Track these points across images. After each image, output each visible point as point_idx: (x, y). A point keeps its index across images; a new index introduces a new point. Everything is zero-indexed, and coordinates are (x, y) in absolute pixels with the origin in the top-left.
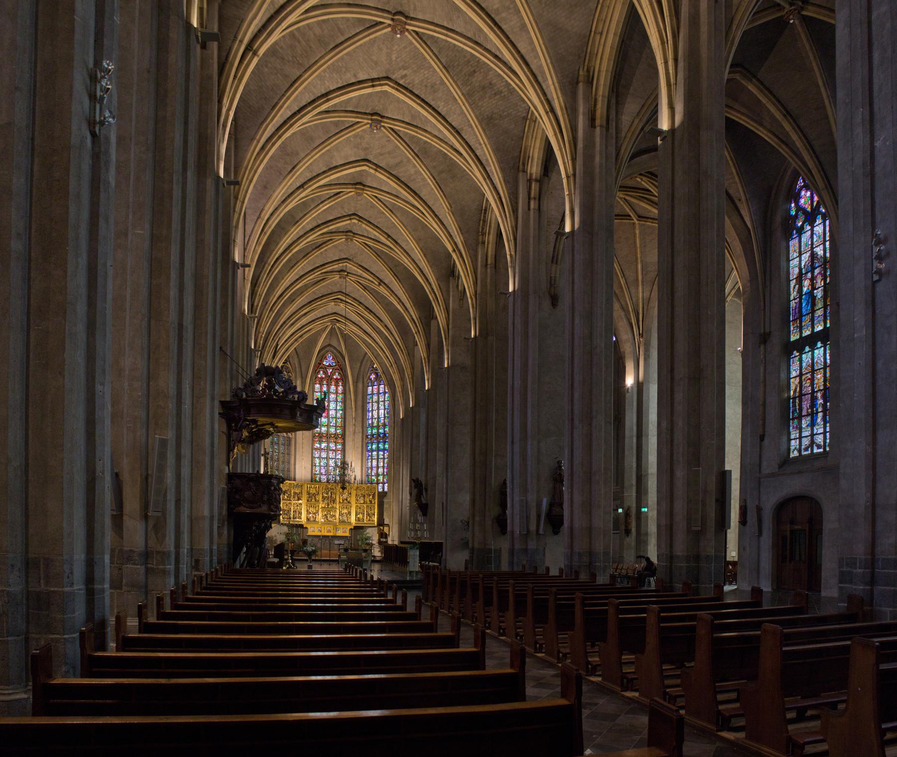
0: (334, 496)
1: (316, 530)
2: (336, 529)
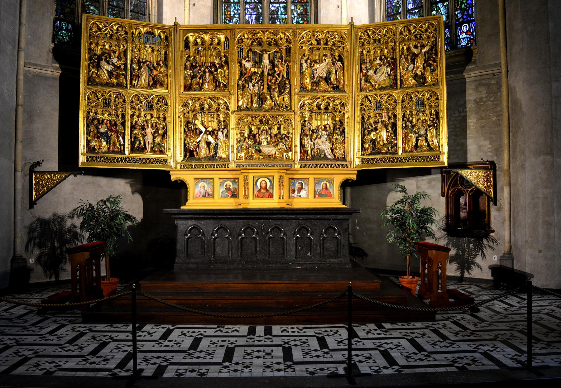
0: (281, 68)
1: (219, 190)
2: (296, 185)
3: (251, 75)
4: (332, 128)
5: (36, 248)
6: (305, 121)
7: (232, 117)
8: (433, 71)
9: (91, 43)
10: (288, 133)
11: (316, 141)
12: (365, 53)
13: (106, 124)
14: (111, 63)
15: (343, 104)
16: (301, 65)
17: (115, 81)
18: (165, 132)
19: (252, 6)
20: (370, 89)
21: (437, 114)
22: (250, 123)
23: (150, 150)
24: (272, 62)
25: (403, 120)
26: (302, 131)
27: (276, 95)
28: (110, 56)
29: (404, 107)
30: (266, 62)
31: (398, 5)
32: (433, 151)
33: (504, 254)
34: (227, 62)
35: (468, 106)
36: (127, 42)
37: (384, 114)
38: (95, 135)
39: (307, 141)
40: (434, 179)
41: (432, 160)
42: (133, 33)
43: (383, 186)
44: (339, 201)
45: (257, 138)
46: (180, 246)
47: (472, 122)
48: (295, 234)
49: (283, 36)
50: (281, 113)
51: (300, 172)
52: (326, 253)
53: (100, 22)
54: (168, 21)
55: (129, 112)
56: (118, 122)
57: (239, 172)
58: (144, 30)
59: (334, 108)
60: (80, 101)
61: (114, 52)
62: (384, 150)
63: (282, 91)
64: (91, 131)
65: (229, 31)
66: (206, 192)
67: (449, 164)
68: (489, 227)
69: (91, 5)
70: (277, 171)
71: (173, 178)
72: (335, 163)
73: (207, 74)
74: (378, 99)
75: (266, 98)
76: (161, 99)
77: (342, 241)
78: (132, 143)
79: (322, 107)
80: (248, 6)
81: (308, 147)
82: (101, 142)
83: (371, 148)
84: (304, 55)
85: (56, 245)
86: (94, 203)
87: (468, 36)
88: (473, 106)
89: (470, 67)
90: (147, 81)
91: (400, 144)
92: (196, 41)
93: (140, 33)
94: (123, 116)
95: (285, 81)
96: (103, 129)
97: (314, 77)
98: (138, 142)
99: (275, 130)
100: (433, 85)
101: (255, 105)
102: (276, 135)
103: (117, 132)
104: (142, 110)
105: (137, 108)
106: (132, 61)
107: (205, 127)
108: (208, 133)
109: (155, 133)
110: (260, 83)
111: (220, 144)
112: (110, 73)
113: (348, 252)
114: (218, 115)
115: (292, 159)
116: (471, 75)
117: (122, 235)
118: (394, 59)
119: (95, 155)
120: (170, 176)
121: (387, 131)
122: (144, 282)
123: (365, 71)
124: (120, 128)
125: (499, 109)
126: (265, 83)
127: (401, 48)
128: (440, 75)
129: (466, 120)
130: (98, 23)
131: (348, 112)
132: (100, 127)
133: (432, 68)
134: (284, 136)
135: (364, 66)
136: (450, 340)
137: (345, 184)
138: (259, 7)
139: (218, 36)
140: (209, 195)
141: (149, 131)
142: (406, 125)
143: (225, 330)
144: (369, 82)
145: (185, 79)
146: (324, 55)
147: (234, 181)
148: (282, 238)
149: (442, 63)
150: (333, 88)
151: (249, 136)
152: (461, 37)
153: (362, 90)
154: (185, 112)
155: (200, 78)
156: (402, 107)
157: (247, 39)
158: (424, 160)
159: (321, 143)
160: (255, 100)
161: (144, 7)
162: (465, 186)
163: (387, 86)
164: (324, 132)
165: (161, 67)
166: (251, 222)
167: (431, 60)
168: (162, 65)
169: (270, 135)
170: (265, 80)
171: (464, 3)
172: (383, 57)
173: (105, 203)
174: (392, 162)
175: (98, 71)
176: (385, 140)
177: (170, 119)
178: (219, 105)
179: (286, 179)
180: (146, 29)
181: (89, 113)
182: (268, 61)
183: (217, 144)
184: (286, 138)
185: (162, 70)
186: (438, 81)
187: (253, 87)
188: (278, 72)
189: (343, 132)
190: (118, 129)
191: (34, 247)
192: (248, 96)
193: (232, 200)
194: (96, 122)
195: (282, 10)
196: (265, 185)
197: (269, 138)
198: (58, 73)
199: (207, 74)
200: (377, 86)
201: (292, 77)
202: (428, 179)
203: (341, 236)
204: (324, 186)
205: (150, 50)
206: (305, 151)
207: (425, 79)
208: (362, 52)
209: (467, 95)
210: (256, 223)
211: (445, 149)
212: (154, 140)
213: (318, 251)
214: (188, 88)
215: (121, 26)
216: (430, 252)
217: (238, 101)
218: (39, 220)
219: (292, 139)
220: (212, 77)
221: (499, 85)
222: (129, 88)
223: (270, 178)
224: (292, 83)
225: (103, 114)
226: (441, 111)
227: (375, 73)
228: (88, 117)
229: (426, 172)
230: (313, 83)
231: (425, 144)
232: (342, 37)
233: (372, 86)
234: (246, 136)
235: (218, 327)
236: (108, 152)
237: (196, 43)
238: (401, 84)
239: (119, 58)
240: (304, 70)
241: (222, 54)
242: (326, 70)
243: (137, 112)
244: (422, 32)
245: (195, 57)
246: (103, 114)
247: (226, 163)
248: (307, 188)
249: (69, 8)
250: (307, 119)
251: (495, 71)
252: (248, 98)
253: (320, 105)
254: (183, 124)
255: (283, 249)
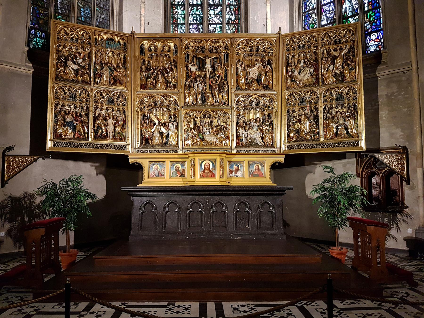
0: (221, 71)
1: (169, 171)
2: (233, 167)
3: (196, 78)
4: (262, 121)
5: (7, 223)
6: (239, 115)
7: (181, 111)
8: (351, 69)
9: (59, 46)
10: (227, 125)
11: (249, 131)
12: (290, 57)
13: (72, 115)
14: (76, 63)
15: (272, 100)
16: (237, 69)
17: (80, 79)
18: (125, 123)
19: (195, 26)
20: (295, 87)
21: (355, 106)
22: (195, 116)
23: (111, 137)
24: (213, 66)
25: (324, 112)
26: (238, 123)
27: (217, 93)
28: (76, 57)
29: (325, 101)
30: (208, 66)
31: (313, 22)
32: (353, 137)
33: (419, 227)
34: (176, 66)
35: (380, 100)
36: (91, 46)
37: (308, 108)
38: (62, 123)
39: (241, 131)
40: (348, 163)
41: (352, 146)
42: (96, 38)
43: (302, 168)
44: (270, 180)
45: (201, 129)
46: (135, 219)
47: (383, 114)
48: (235, 208)
49: (222, 44)
50: (221, 108)
51: (237, 156)
52: (262, 225)
53: (68, 28)
54: (127, 30)
55: (92, 106)
56: (83, 114)
57: (187, 156)
58: (106, 37)
59: (264, 104)
60: (49, 94)
61: (80, 54)
62: (308, 137)
63: (222, 90)
64: (58, 121)
65: (177, 39)
66: (159, 172)
67: (366, 149)
68: (403, 204)
69: (63, 19)
70: (218, 155)
71: (131, 161)
72: (265, 149)
73: (160, 76)
74: (303, 95)
75: (208, 96)
76: (121, 95)
77: (276, 215)
78: (96, 132)
79: (254, 103)
80: (191, 27)
81: (243, 135)
82: (67, 130)
83: (295, 137)
84: (239, 61)
85: (26, 219)
86: (57, 182)
87: (376, 43)
88: (385, 100)
89: (381, 67)
90: (108, 79)
91: (322, 132)
92: (149, 48)
93: (102, 39)
94: (88, 108)
95: (224, 82)
96: (69, 119)
97: (247, 79)
98: (100, 131)
99: (216, 123)
100: (352, 81)
101: (199, 102)
102: (216, 127)
103: (82, 122)
104: (105, 104)
105: (99, 101)
106: (95, 63)
107: (158, 120)
108: (161, 124)
109: (115, 124)
110: (203, 84)
111: (171, 133)
112: (76, 71)
113: (282, 225)
114: (169, 110)
115: (229, 146)
116: (382, 73)
117: (82, 211)
118: (316, 61)
119: (62, 141)
120: (128, 159)
121: (310, 123)
122: (97, 257)
123: (290, 73)
124: (85, 118)
125: (409, 102)
126: (208, 84)
127: (322, 51)
128: (357, 73)
129: (378, 112)
130: (66, 29)
131: (276, 107)
132: (66, 117)
133: (350, 67)
134: (223, 127)
135: (289, 68)
136: (384, 309)
137: (275, 167)
138: (200, 27)
139: (168, 44)
140: (161, 175)
141: (111, 122)
142: (326, 116)
143: (176, 309)
144: (295, 81)
145: (141, 79)
146: (256, 61)
147: (183, 164)
148: (224, 211)
149: (359, 63)
150: (264, 87)
151: (194, 127)
152: (370, 44)
153: (288, 88)
154: (141, 107)
155: (153, 79)
156: (324, 102)
157: (193, 47)
158: (344, 146)
159: (253, 134)
160: (199, 98)
161: (107, 24)
162: (377, 168)
163: (310, 84)
164: (255, 124)
165: (120, 69)
166: (197, 198)
167: (349, 61)
168: (121, 67)
169: (212, 126)
170: (207, 81)
171: (372, 16)
172: (306, 60)
173: (67, 182)
174: (314, 147)
175: (65, 69)
176: (308, 129)
177: (128, 113)
178: (169, 101)
179: (225, 161)
180: (107, 35)
181: (57, 106)
182: (209, 66)
183: (168, 134)
184: (225, 129)
185: (122, 71)
186: (356, 78)
187: (198, 87)
188: (218, 75)
189: (271, 123)
190: (82, 119)
191: (5, 221)
192: (193, 94)
193: (181, 179)
194: (63, 113)
195: (219, 30)
196: (208, 167)
197: (211, 129)
198: (31, 72)
199: (160, 76)
200: (301, 84)
201: (229, 79)
202: (343, 163)
203: (275, 210)
204: (257, 168)
205: (111, 54)
206: (240, 139)
207: (344, 76)
208: (288, 57)
209: (379, 91)
210: (202, 199)
211: (363, 136)
212: (115, 130)
213: (256, 223)
214: (144, 87)
215: (85, 32)
216: (368, 228)
217: (185, 99)
218: (10, 197)
219: (229, 130)
220: (163, 79)
221: (409, 81)
222: (92, 85)
223: (213, 161)
224: (229, 84)
225: (69, 106)
226: (359, 103)
227: (299, 73)
228: (56, 108)
229: (342, 156)
230: (246, 84)
231: (344, 132)
232: (271, 45)
233: (297, 84)
234: (192, 127)
235: (169, 304)
236: (74, 138)
237: (150, 50)
238: (323, 82)
239: (84, 59)
240: (239, 72)
241: (172, 59)
242: (257, 73)
243: (100, 105)
244: (341, 37)
245: (149, 61)
246: (69, 106)
247: (176, 149)
248: (242, 170)
249: (43, 19)
250: (241, 113)
251: (406, 69)
252: (193, 96)
253: (252, 101)
254: (140, 117)
255: (225, 221)
